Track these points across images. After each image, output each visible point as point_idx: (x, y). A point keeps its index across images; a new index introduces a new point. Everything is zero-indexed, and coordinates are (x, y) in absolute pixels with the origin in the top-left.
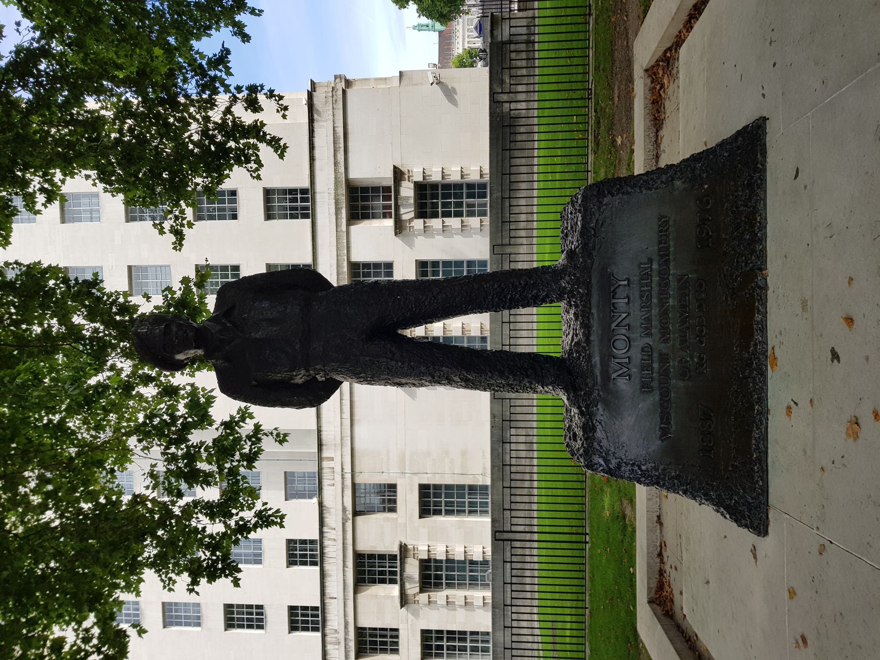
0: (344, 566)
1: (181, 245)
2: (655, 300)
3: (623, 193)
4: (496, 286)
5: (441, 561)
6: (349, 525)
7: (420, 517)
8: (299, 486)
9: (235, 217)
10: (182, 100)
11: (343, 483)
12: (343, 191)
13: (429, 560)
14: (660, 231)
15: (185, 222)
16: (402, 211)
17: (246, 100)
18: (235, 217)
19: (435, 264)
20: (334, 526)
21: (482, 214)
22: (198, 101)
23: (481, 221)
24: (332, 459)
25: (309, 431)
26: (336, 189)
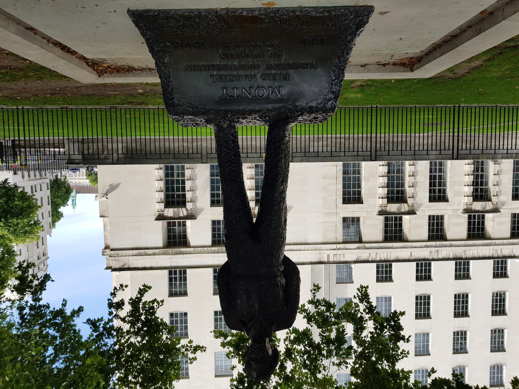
0: (392, 248)
1: (203, 347)
2: (235, 73)
3: (172, 92)
4: (227, 165)
5: (388, 190)
6: (367, 245)
7: (362, 203)
8: (345, 275)
9: (186, 314)
10: (117, 347)
11: (343, 249)
12: (170, 250)
13: (388, 198)
14: (194, 70)
15: (189, 345)
17: (117, 309)
18: (186, 314)
19: (212, 195)
20: (368, 254)
21: (183, 168)
22: (118, 338)
23: (187, 169)
24: (328, 255)
25: (312, 270)
26: (169, 254)
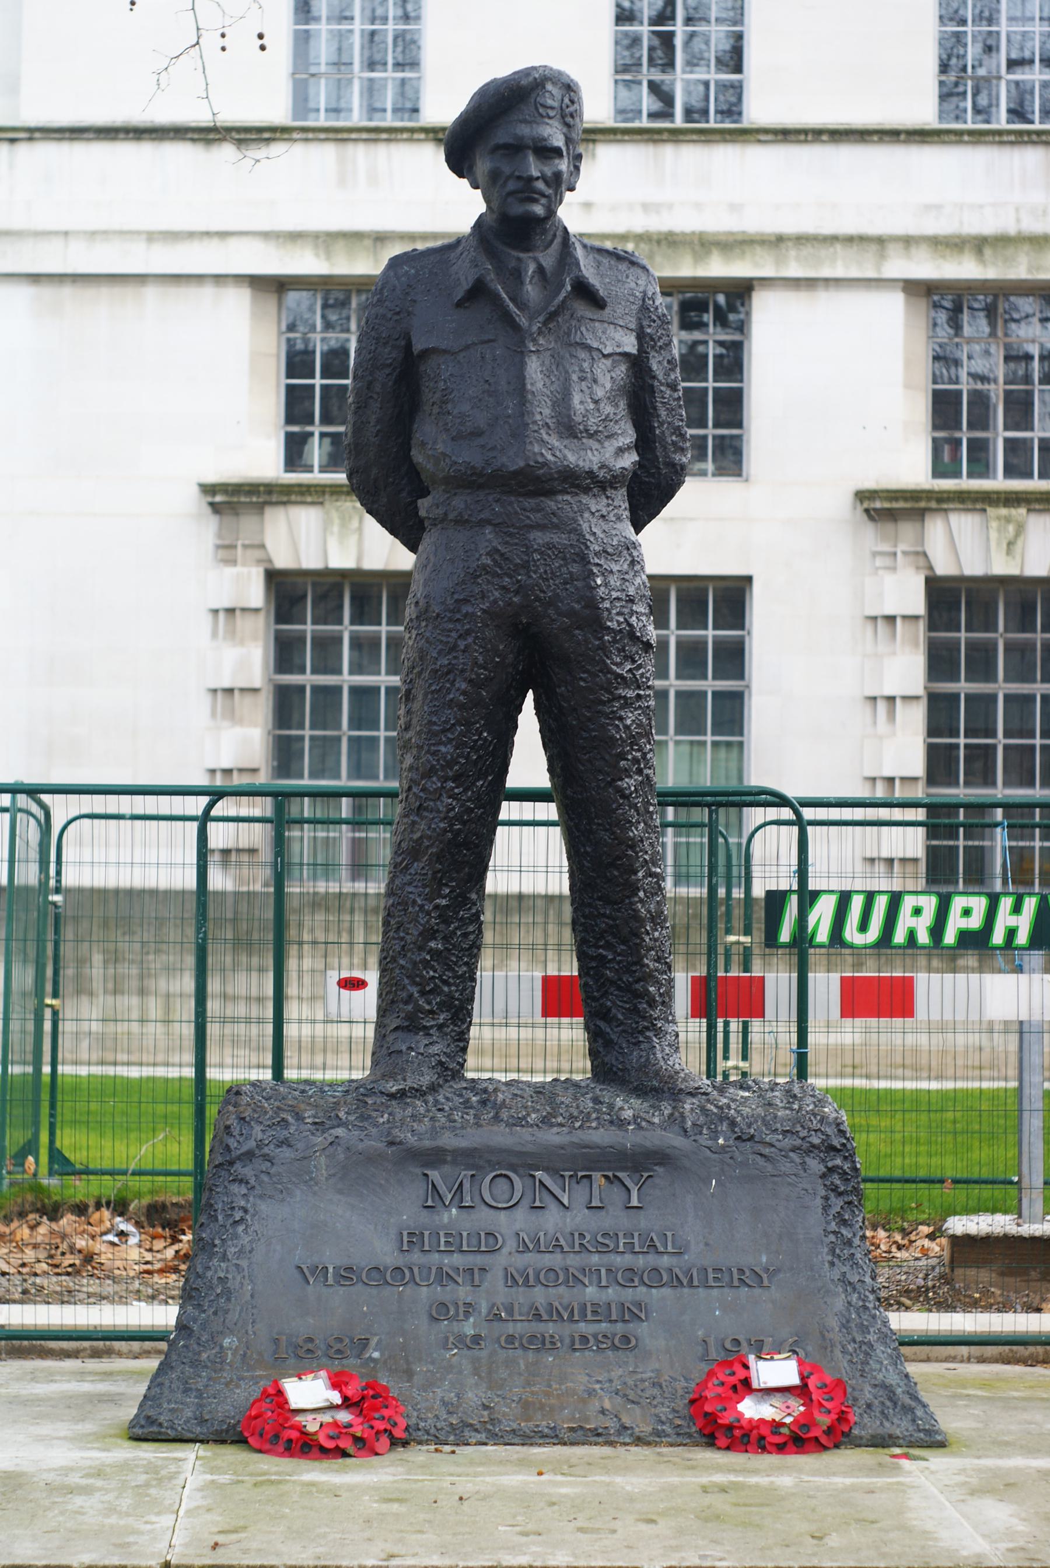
3: (826, 1198)
14: (741, 1271)
16: (964, 524)
19: (733, 658)
